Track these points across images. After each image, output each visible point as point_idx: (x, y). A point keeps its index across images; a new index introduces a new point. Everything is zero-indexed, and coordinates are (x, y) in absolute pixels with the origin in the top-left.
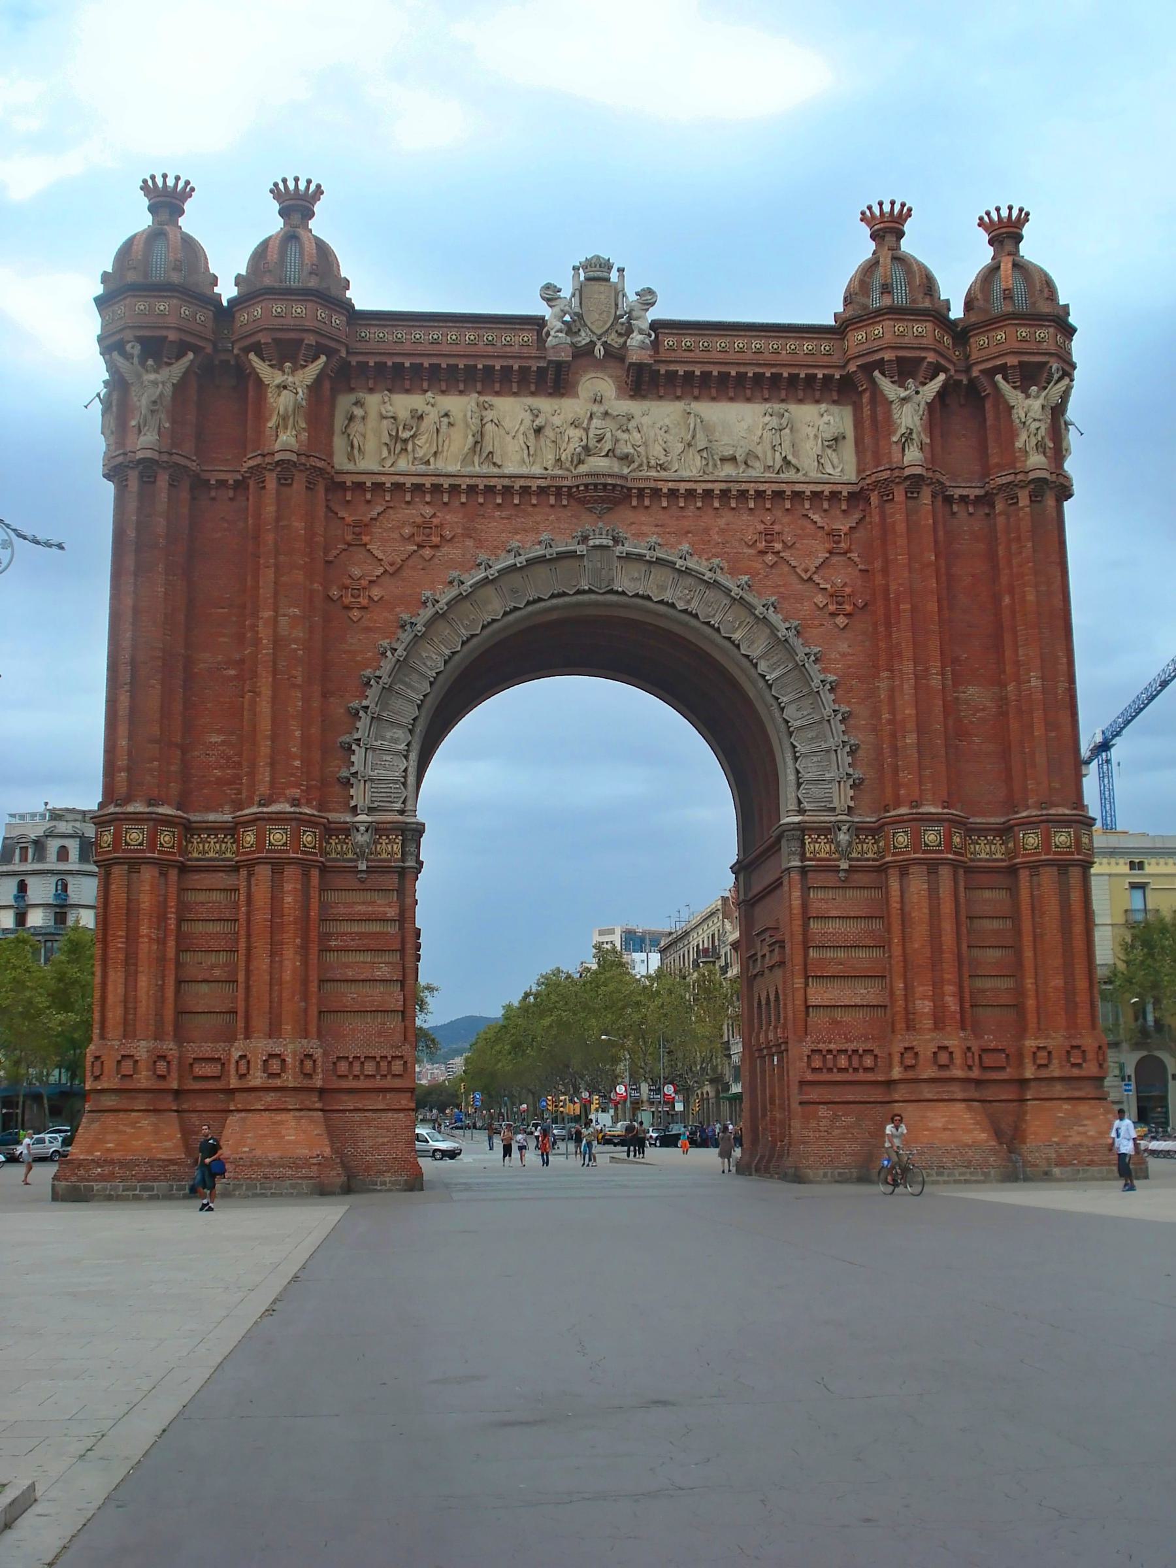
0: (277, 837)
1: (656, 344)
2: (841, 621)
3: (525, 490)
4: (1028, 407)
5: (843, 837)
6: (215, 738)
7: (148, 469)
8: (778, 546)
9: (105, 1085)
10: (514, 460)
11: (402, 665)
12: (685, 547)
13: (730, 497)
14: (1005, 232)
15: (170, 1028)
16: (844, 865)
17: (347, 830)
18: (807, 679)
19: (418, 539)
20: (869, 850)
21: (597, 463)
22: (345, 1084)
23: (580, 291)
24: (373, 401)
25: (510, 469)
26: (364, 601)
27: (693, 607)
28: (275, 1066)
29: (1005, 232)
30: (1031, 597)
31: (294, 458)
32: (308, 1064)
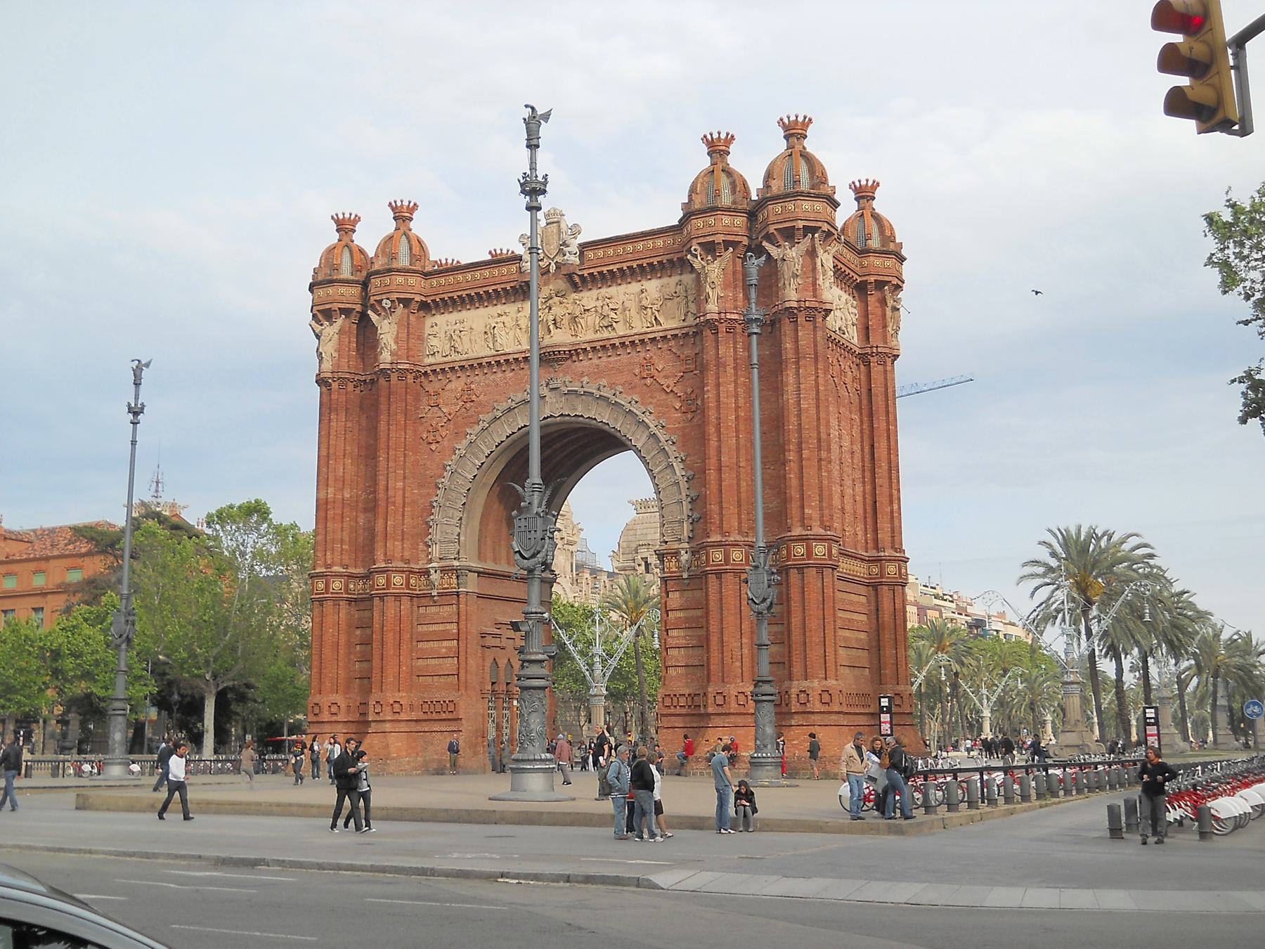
0: (381, 580)
2: (689, 416)
5: (684, 557)
8: (656, 373)
9: (338, 718)
14: (794, 131)
15: (341, 688)
16: (685, 576)
17: (426, 573)
19: (464, 398)
22: (425, 717)
26: (439, 439)
28: (378, 706)
29: (794, 131)
31: (388, 366)
32: (396, 705)
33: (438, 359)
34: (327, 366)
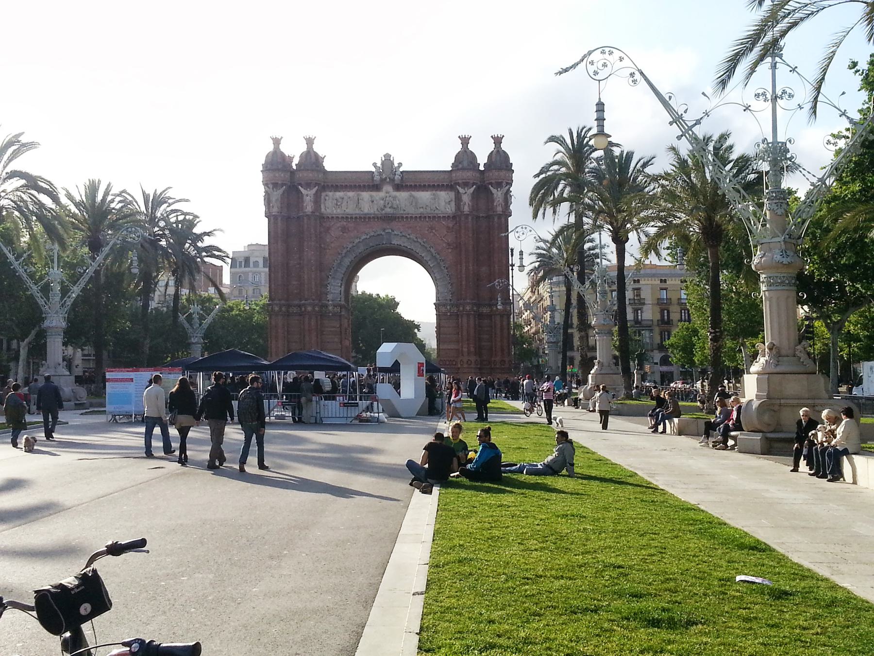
1: (402, 178)
3: (369, 218)
4: (498, 194)
6: (294, 283)
7: (275, 217)
10: (367, 208)
11: (340, 264)
12: (410, 232)
13: (422, 217)
14: (498, 141)
18: (440, 267)
20: (455, 310)
21: (388, 210)
23: (383, 163)
24: (331, 194)
25: (366, 211)
27: (412, 247)
30: (496, 245)
33: (329, 211)
34: (275, 210)
